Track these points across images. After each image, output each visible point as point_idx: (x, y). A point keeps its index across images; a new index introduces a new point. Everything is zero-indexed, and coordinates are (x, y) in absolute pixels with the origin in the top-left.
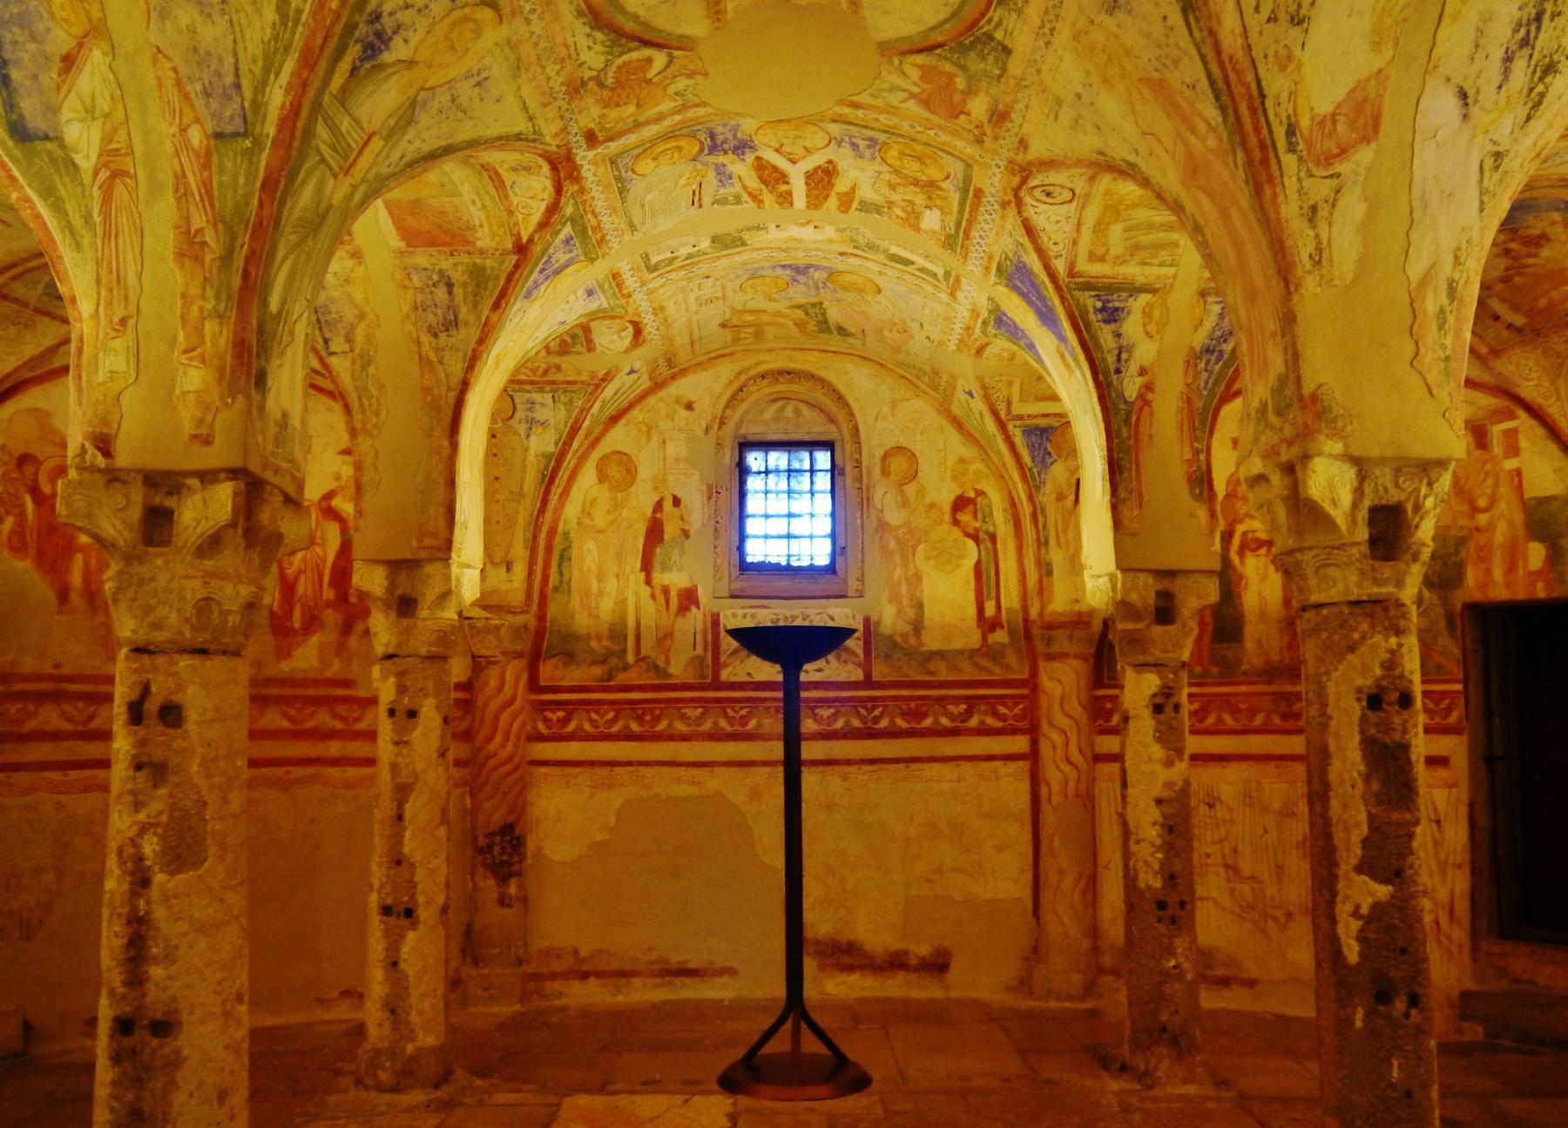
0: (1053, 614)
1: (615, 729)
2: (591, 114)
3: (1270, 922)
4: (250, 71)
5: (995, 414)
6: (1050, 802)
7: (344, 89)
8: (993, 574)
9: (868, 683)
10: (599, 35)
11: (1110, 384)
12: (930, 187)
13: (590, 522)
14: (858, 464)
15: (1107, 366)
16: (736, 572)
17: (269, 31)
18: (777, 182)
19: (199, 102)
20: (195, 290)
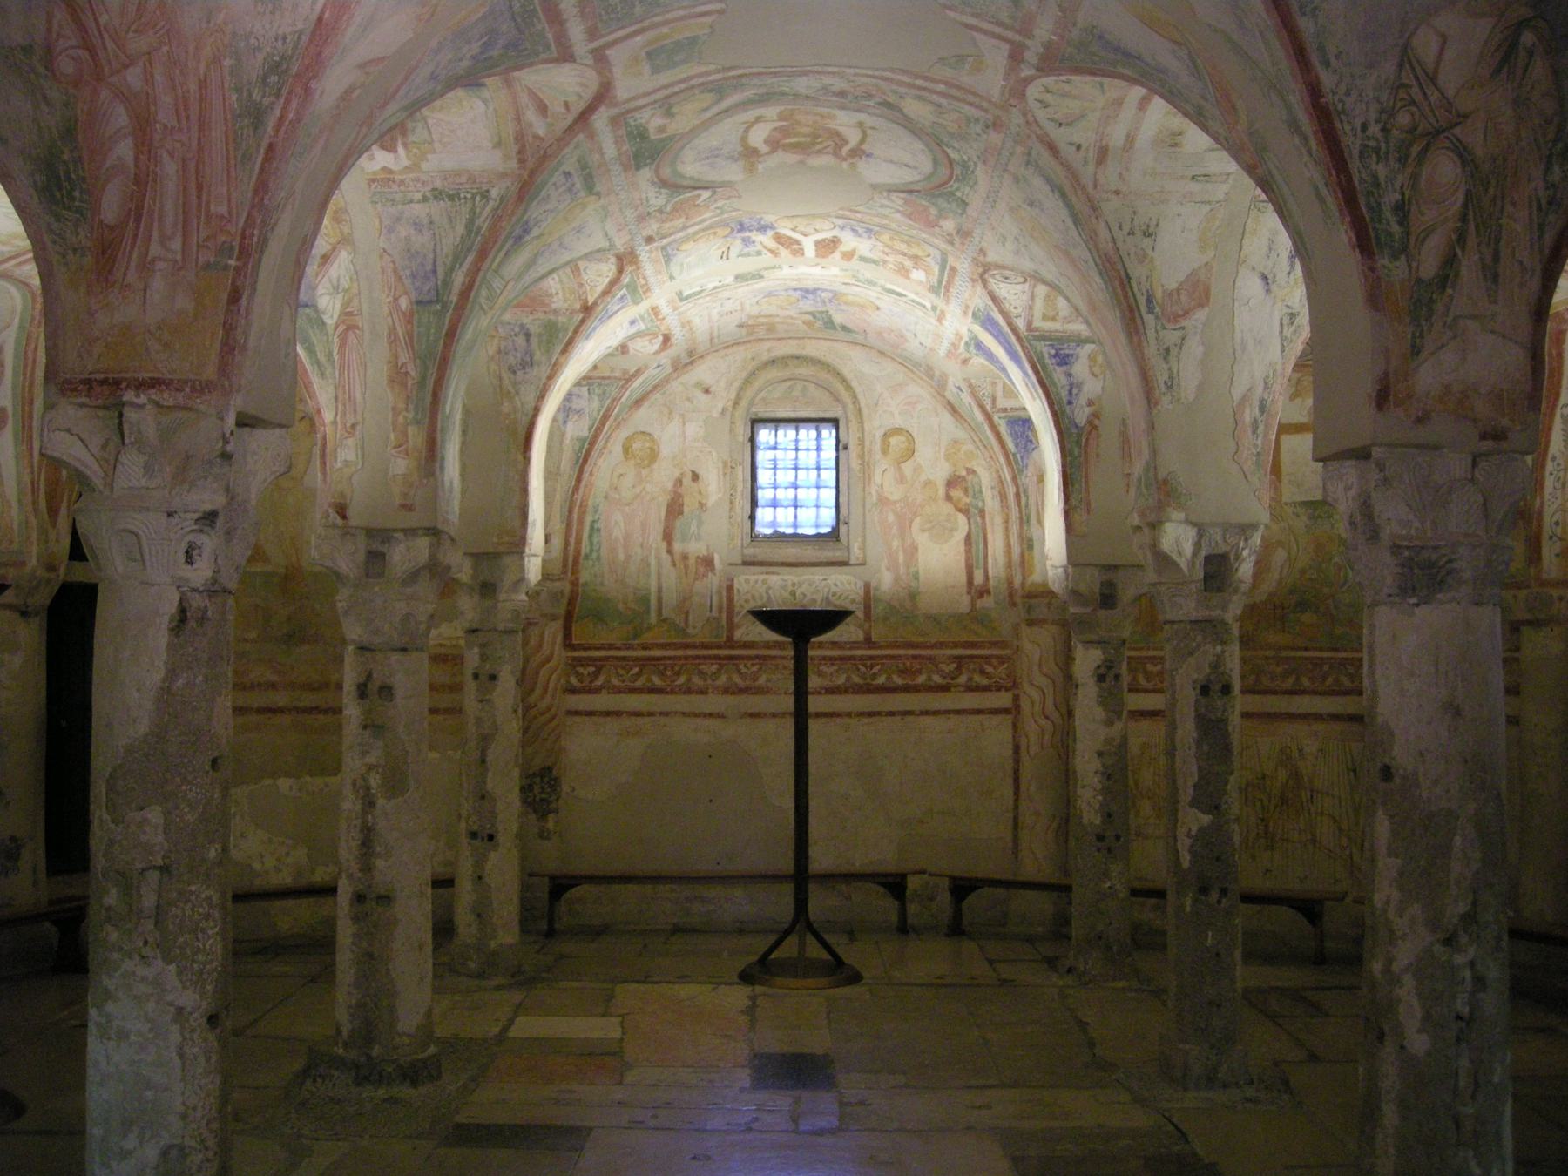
0: (1033, 584)
1: (639, 683)
2: (653, 227)
4: (444, 262)
5: (982, 407)
6: (1028, 752)
7: (499, 265)
8: (981, 546)
9: (868, 642)
10: (663, 191)
11: (1063, 413)
12: (915, 259)
13: (617, 496)
14: (862, 441)
15: (1061, 399)
16: (749, 540)
17: (458, 239)
18: (792, 244)
19: (408, 282)
20: (401, 405)
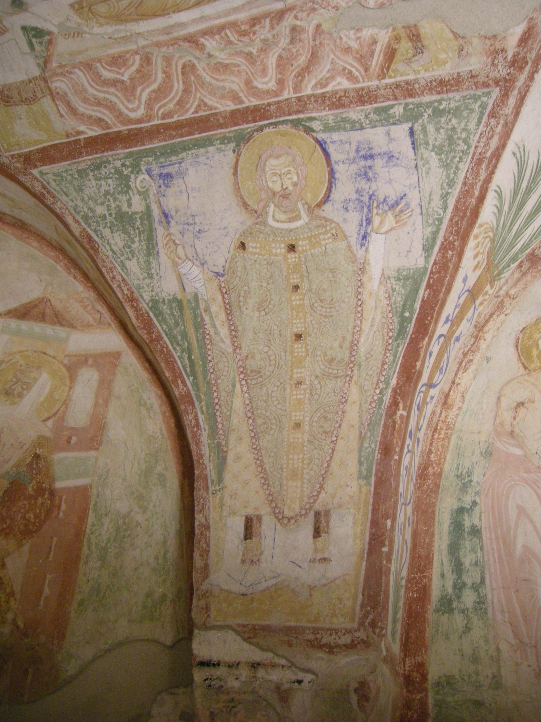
13: (518, 452)
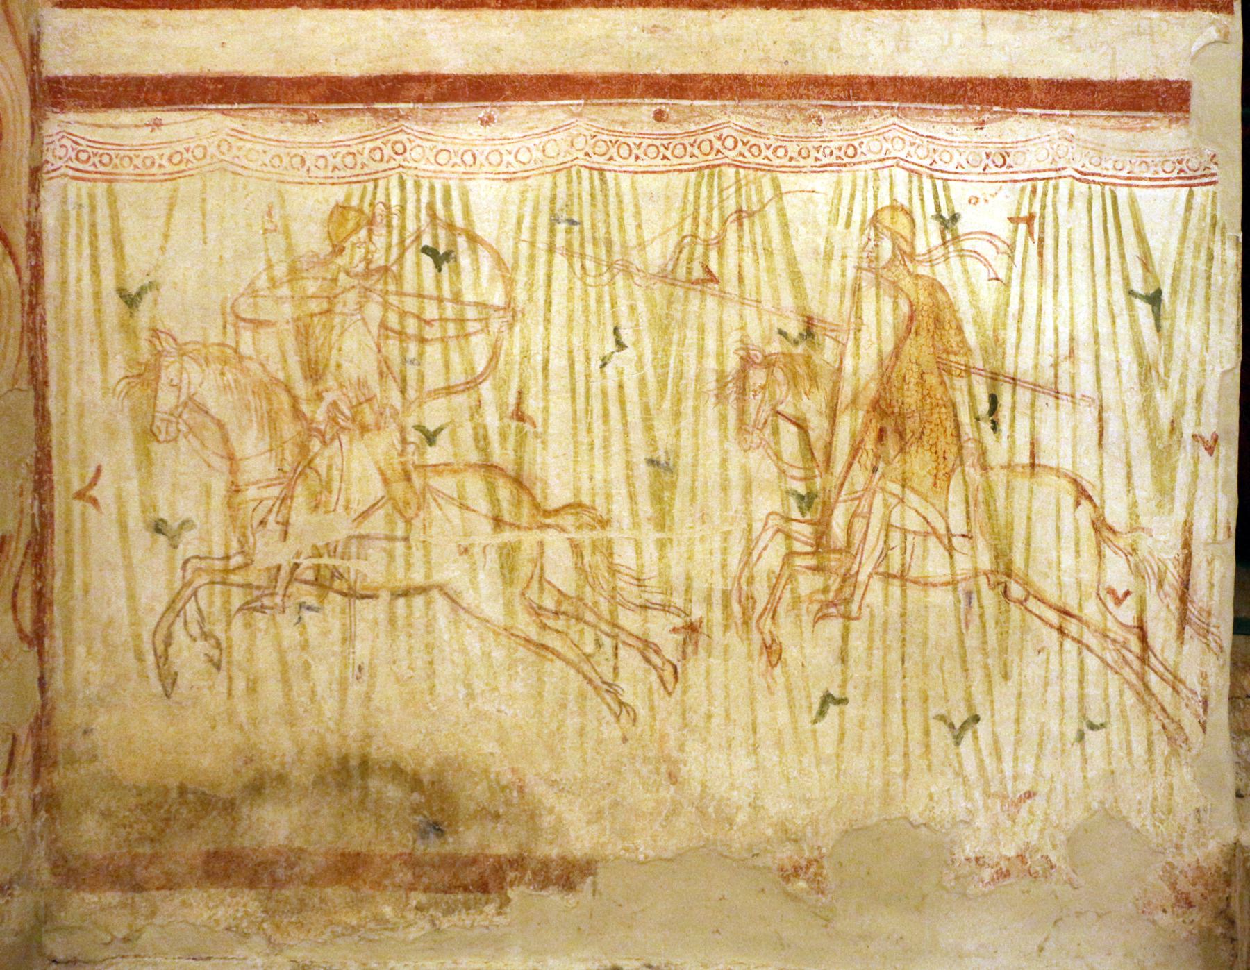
3: (630, 659)
